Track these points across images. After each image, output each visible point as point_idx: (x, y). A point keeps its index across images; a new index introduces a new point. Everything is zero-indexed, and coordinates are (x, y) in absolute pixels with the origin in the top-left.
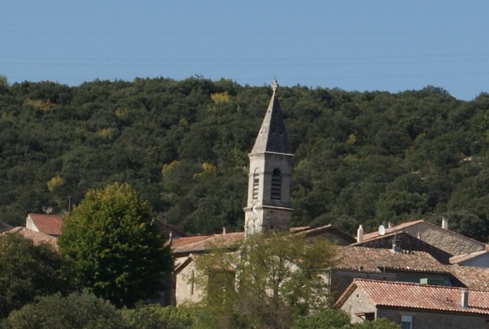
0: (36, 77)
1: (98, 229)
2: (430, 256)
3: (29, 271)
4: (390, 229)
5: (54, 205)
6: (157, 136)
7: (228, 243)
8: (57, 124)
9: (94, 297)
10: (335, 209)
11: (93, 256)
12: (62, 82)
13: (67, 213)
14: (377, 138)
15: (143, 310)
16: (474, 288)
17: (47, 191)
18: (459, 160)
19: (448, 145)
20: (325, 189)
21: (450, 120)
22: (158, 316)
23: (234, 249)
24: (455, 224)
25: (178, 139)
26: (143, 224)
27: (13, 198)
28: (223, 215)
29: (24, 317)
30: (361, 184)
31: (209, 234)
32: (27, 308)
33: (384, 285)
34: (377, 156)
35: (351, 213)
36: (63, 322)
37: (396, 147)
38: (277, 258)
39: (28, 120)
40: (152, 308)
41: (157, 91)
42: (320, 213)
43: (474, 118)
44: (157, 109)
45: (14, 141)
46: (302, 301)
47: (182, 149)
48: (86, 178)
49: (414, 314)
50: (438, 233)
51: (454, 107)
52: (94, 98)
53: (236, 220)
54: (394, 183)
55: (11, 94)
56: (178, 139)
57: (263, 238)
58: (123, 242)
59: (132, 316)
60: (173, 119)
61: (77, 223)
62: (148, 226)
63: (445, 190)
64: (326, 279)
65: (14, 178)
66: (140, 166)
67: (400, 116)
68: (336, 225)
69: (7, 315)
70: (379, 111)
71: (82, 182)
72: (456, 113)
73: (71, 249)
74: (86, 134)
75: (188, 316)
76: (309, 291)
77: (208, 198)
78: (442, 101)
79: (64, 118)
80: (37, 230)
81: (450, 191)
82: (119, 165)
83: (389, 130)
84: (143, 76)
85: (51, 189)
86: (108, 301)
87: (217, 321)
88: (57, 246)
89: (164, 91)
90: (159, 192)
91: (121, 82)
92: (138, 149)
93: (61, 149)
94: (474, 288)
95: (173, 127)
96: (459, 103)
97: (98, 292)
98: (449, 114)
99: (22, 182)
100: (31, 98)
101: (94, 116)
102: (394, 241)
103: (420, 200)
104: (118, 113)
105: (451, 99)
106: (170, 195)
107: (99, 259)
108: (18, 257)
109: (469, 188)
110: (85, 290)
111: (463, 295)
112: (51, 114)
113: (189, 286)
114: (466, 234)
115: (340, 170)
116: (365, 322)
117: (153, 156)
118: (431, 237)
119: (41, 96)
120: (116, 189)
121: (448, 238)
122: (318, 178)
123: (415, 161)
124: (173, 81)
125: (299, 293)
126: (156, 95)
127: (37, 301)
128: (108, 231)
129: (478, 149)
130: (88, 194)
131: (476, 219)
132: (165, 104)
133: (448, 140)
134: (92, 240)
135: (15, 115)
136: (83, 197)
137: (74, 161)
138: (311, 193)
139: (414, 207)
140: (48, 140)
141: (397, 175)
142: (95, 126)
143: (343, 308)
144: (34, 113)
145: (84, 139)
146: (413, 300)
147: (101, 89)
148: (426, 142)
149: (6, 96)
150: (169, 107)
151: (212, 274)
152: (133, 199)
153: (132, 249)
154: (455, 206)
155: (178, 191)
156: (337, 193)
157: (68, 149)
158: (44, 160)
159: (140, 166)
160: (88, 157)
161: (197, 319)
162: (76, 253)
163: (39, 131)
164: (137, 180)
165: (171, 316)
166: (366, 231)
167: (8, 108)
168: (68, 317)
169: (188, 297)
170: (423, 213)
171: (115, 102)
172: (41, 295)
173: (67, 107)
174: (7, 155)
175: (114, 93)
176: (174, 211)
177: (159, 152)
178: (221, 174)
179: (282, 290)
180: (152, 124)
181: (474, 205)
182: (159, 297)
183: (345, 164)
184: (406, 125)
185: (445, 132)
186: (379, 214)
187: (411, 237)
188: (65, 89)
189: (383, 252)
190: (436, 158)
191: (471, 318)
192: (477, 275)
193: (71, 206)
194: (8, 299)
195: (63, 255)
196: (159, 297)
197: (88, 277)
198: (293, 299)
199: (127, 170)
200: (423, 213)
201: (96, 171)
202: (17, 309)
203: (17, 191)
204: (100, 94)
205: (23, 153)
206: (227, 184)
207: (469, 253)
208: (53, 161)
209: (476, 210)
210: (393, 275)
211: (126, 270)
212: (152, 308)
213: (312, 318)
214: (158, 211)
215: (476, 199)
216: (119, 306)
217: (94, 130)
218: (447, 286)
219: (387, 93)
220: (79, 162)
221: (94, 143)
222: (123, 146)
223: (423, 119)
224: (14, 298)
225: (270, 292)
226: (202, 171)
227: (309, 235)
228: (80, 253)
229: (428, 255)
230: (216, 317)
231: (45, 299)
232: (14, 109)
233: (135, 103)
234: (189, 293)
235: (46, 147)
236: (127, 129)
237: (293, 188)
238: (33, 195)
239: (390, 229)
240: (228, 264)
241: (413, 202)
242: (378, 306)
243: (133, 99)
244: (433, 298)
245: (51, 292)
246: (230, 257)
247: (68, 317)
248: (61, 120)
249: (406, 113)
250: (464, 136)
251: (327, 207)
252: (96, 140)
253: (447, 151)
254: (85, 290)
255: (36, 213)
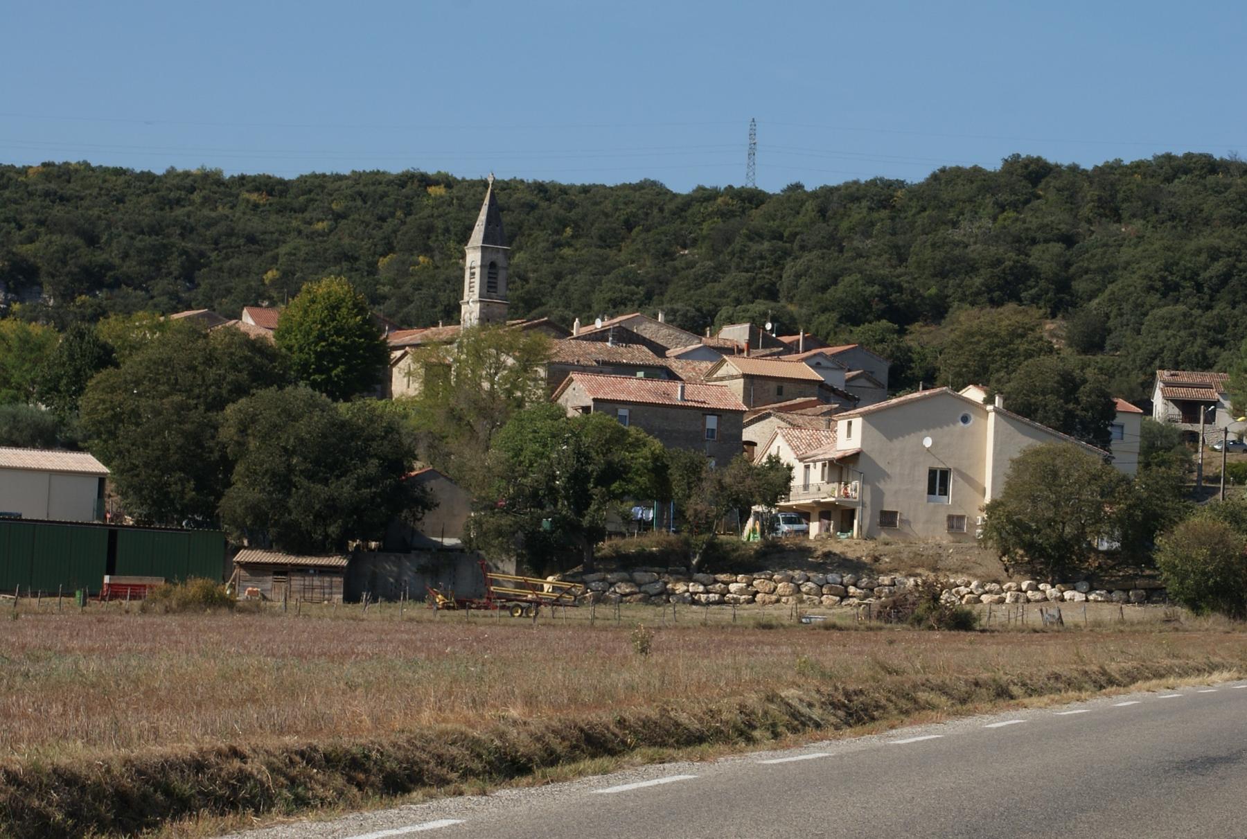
0: (252, 170)
1: (314, 322)
2: (647, 350)
3: (245, 365)
4: (607, 322)
5: (270, 298)
6: (374, 229)
7: (444, 337)
8: (273, 217)
9: (310, 390)
10: (552, 302)
11: (310, 349)
12: (278, 175)
13: (283, 306)
14: (594, 231)
15: (359, 403)
16: (691, 381)
17: (264, 284)
18: (675, 253)
19: (664, 239)
20: (541, 283)
21: (666, 213)
22: (374, 409)
23: (451, 343)
24: (671, 318)
25: (395, 232)
26: (359, 318)
27: (229, 291)
28: (440, 308)
29: (240, 411)
30: (578, 277)
31: (426, 327)
32: (243, 401)
33: (600, 378)
34: (593, 248)
35: (567, 306)
36: (279, 415)
37: (613, 240)
38: (493, 351)
39: (244, 213)
40: (368, 401)
41: (373, 184)
42: (536, 307)
43: (690, 211)
44: (374, 202)
45: (231, 233)
46: (519, 394)
47: (398, 243)
48: (302, 272)
49: (631, 407)
50: (654, 327)
51: (671, 200)
52: (310, 191)
53: (452, 313)
54: (610, 276)
55: (227, 187)
56: (395, 232)
57: (479, 331)
58: (339, 335)
59: (348, 410)
60: (390, 212)
61: (293, 316)
62: (364, 320)
63: (661, 283)
64: (542, 372)
65: (231, 270)
66: (356, 259)
67: (617, 209)
68: (553, 318)
69: (223, 409)
70: (596, 204)
71: (298, 275)
72: (672, 206)
73: (287, 342)
74: (302, 227)
75: (405, 409)
76: (525, 384)
77: (424, 291)
78: (659, 194)
79: (280, 211)
80: (253, 323)
81: (667, 284)
82: (335, 258)
83: (605, 223)
84: (360, 169)
85: (267, 282)
86: (324, 395)
87: (433, 415)
88: (273, 340)
89: (380, 183)
90: (375, 285)
91: (337, 174)
92: (354, 242)
93: (277, 242)
94: (691, 381)
95: (389, 220)
96: (675, 196)
97: (314, 385)
98: (665, 207)
99: (238, 275)
100: (248, 191)
101: (310, 208)
102: (610, 334)
103: (636, 294)
104: (334, 206)
105: (668, 192)
106: (387, 289)
107: (315, 352)
108: (233, 350)
109: (686, 282)
110: (302, 383)
111: (679, 389)
112: (267, 207)
113: (406, 380)
114: (683, 327)
115: (556, 263)
116: (581, 415)
117: (369, 249)
118: (648, 330)
119: (257, 189)
120: (332, 282)
121: (665, 331)
122: (535, 271)
123: (631, 254)
124: (389, 174)
125: (515, 386)
126: (372, 188)
127: (254, 395)
128: (324, 324)
129: (695, 242)
130: (304, 287)
131: (692, 312)
132: (381, 198)
133: (666, 234)
134: (308, 334)
135: (231, 208)
136: (299, 290)
137: (290, 254)
138: (527, 286)
139: (630, 300)
140: (264, 233)
141: (613, 268)
142: (311, 219)
143: (559, 401)
144: (250, 206)
145: (300, 232)
146: (630, 393)
147: (317, 182)
148: (643, 235)
149: (222, 189)
150: (385, 200)
151: (428, 367)
152: (349, 292)
153: (348, 342)
154: (672, 299)
155: (394, 283)
156: (553, 286)
157: (284, 242)
158: (260, 253)
159: (356, 259)
160: (304, 249)
161: (414, 413)
162: (292, 346)
163: (254, 224)
164: (353, 273)
165: (387, 410)
166: (582, 324)
167: (225, 201)
168: (284, 410)
169: (405, 390)
170: (640, 306)
171: (331, 195)
172: (257, 388)
173: (283, 200)
174: (224, 248)
175: (330, 186)
176: (390, 304)
177: (376, 245)
178: (437, 267)
179: (498, 383)
180: (368, 218)
181: (691, 299)
182: (375, 390)
183: (562, 258)
184: (622, 217)
185: (661, 225)
186: (596, 307)
187: (627, 330)
188: (281, 182)
189: (599, 345)
190: (653, 251)
191: (689, 411)
192: (694, 369)
193: (288, 301)
194: (224, 392)
195: (280, 349)
196: (375, 390)
197: (304, 371)
198: (509, 393)
199: (344, 263)
200: (640, 306)
201: (312, 264)
202: (233, 402)
203: (233, 284)
204: (316, 187)
205: (239, 246)
206: (442, 277)
207: (686, 346)
208: (269, 254)
209: (693, 303)
210: (609, 369)
211: (343, 363)
212: (368, 401)
213: (528, 411)
214: (374, 305)
215: (692, 292)
216: (335, 400)
217: (310, 223)
218: (663, 379)
219: (604, 186)
220: (295, 255)
221: (311, 236)
222: (339, 239)
223: (640, 212)
224: (230, 391)
225: (486, 385)
226: (418, 263)
227: (525, 328)
228: (296, 346)
229: (645, 348)
230: (432, 411)
231: (261, 392)
232: (230, 202)
233: (351, 196)
234: (405, 386)
235: (262, 240)
236: (344, 221)
237: (509, 281)
238: (249, 288)
239: (607, 322)
240: (444, 357)
241: (629, 296)
242: (594, 400)
243: (349, 192)
244: (649, 391)
245: (268, 385)
246: (447, 350)
247: (284, 410)
248: (277, 213)
249: (622, 206)
250: (681, 229)
251: (544, 300)
252: (313, 233)
253: (664, 243)
254: (302, 383)
255: (252, 306)
